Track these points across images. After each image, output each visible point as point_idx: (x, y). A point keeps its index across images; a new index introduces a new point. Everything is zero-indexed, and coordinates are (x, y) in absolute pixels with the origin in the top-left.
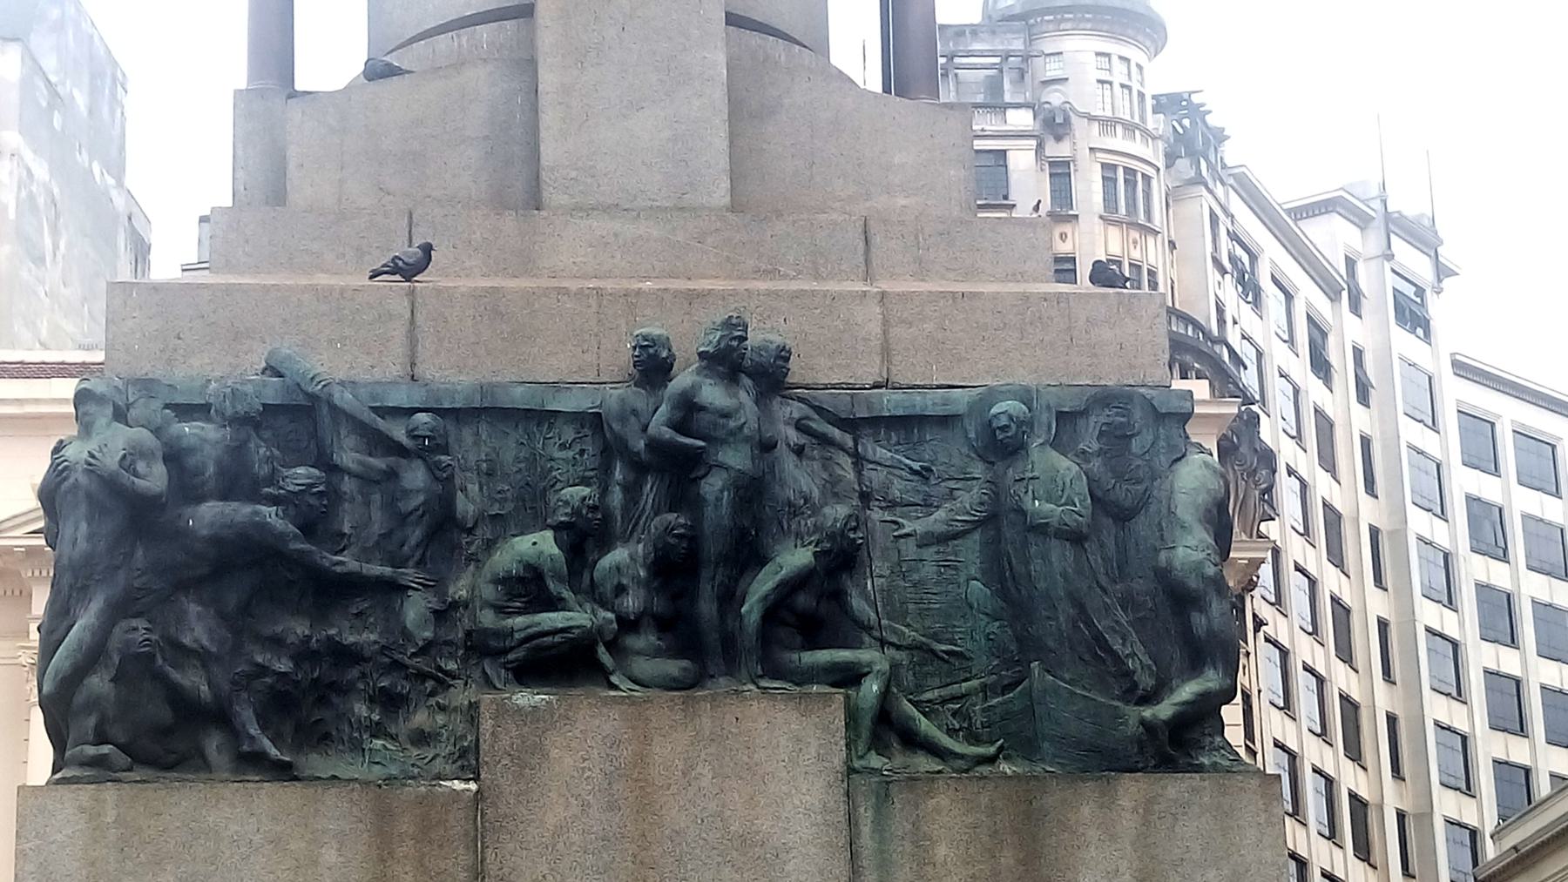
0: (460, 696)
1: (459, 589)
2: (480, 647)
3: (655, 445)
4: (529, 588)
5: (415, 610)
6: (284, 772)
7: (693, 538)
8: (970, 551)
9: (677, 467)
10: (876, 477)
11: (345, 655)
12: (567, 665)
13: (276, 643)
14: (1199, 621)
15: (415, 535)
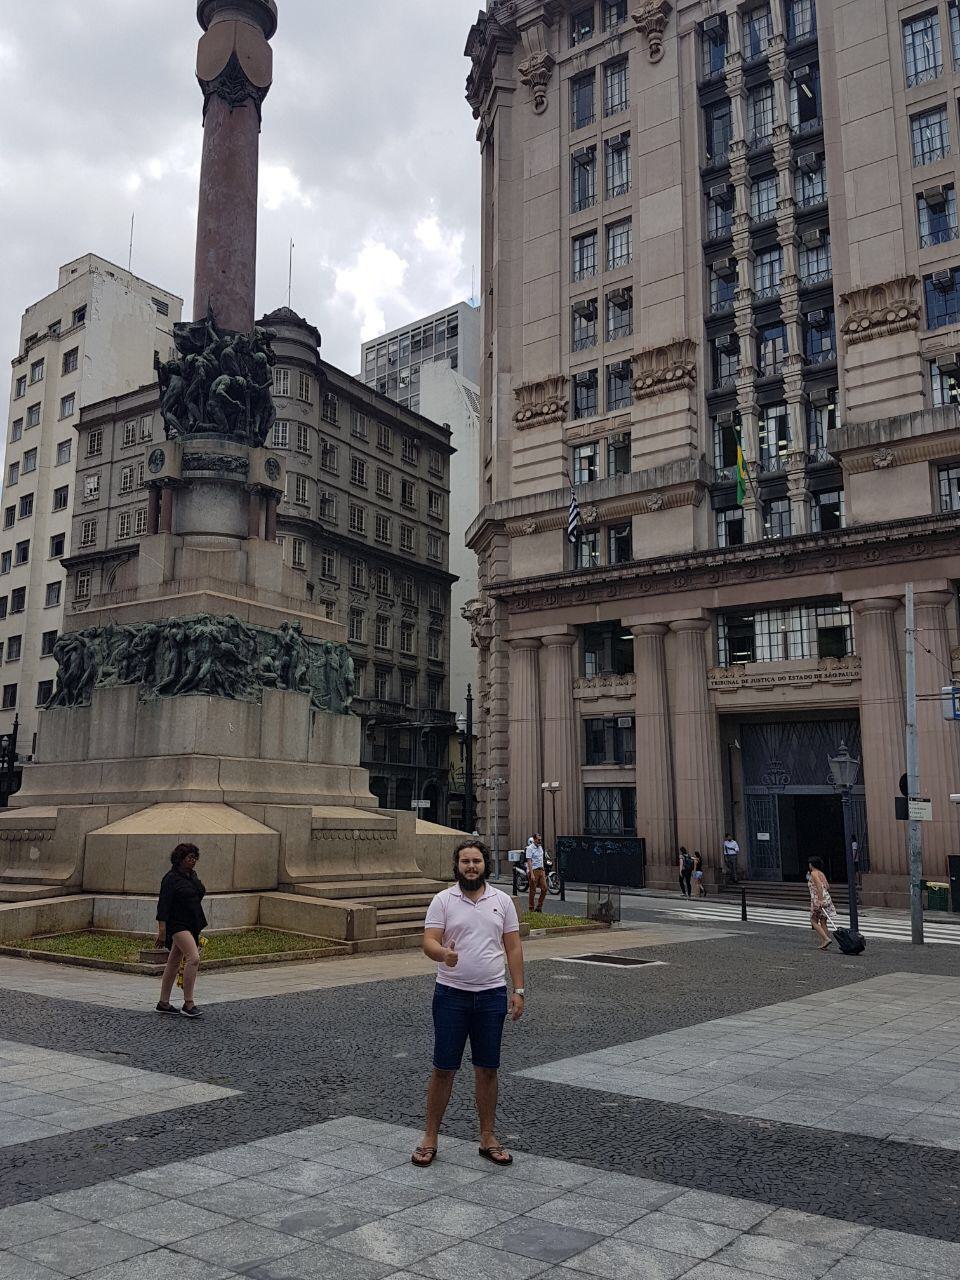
0: (256, 686)
1: (256, 665)
2: (259, 677)
3: (286, 644)
4: (268, 668)
5: (249, 668)
6: (233, 698)
7: (290, 662)
8: (322, 670)
9: (288, 648)
10: (311, 654)
11: (239, 676)
12: (271, 683)
13: (231, 672)
14: (350, 688)
15: (250, 654)
